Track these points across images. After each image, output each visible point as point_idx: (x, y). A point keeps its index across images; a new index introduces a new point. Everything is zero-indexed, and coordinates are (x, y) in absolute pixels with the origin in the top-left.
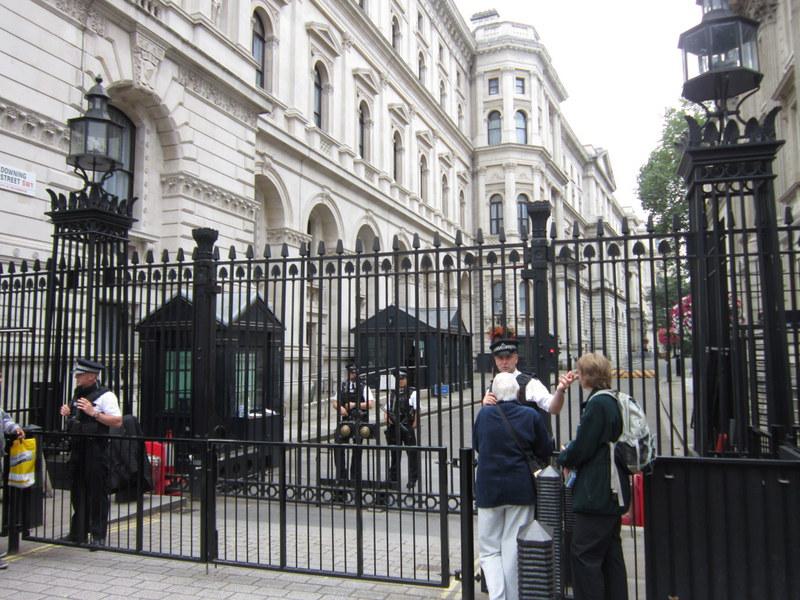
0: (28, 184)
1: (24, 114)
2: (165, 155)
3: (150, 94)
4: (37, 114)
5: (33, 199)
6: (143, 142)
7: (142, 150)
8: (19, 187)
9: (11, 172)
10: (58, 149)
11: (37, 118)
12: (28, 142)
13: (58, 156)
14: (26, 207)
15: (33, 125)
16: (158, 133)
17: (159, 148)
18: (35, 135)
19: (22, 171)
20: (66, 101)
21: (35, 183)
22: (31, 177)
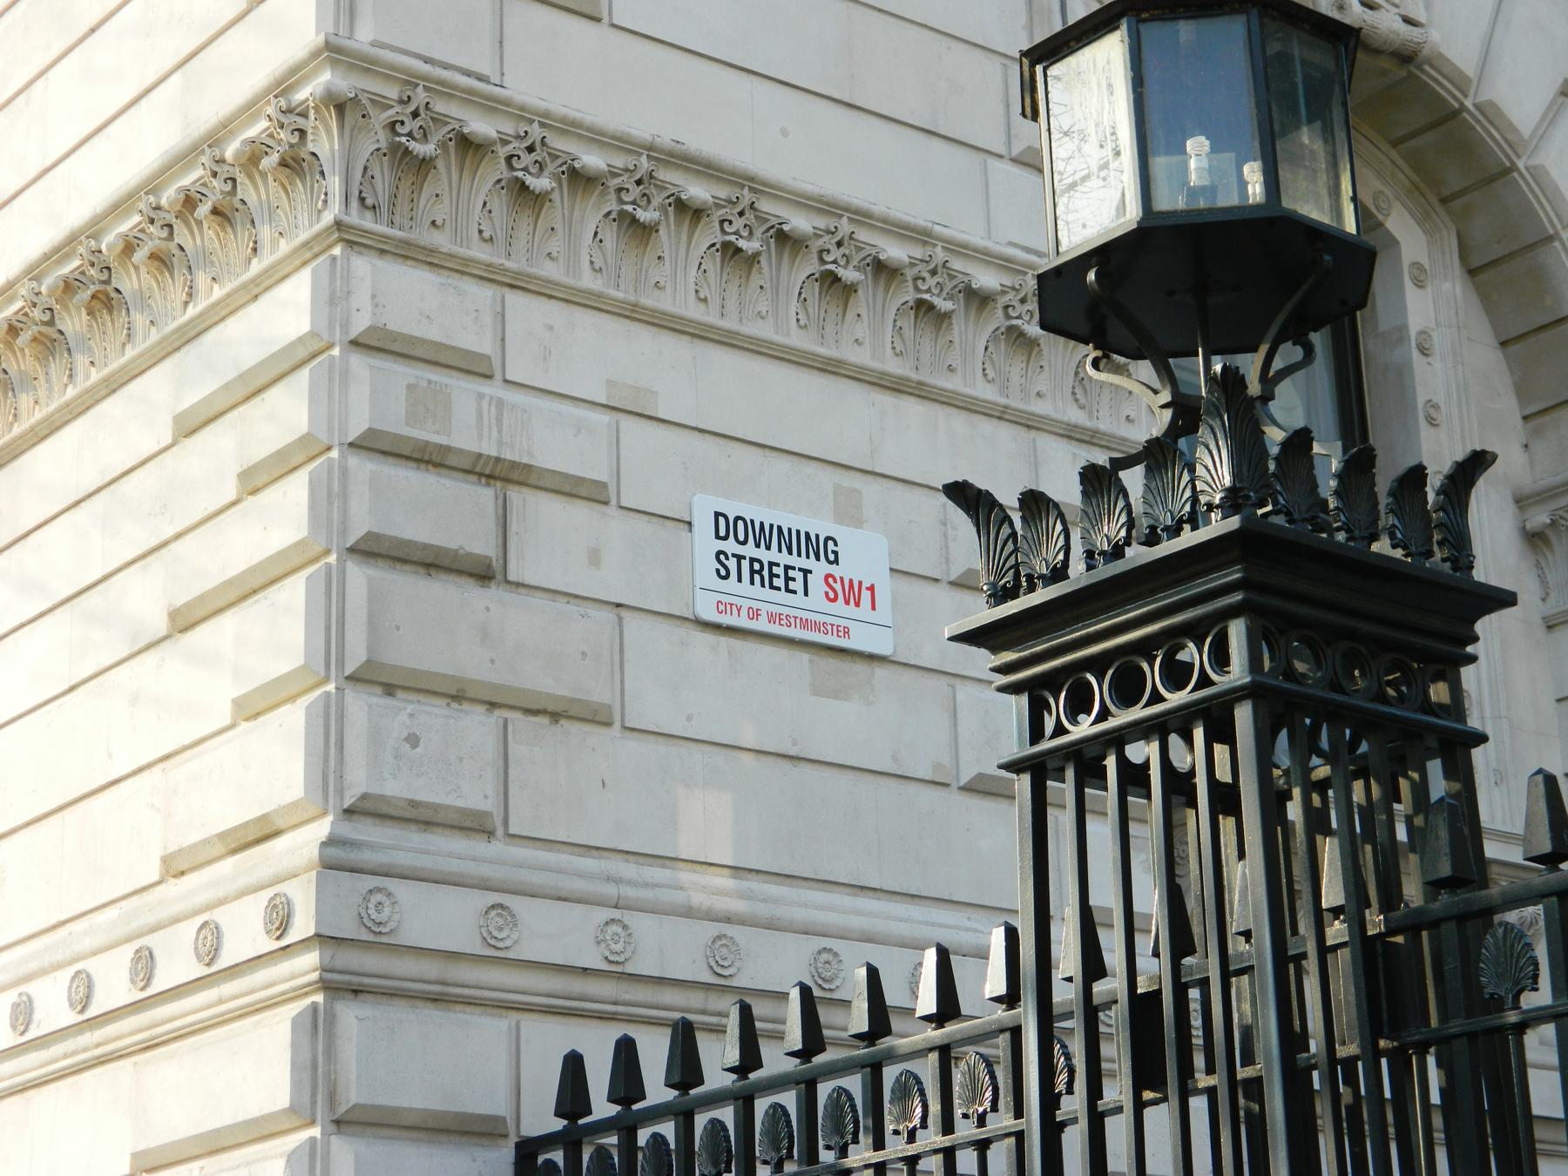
0: (852, 593)
1: (800, 222)
2: (1522, 392)
3: (1406, 57)
4: (862, 216)
5: (881, 672)
6: (1401, 331)
7: (1402, 376)
8: (813, 605)
9: (762, 534)
10: (985, 392)
11: (863, 235)
12: (831, 368)
13: (986, 426)
14: (850, 723)
15: (849, 275)
16: (1472, 272)
17: (1486, 356)
18: (862, 330)
19: (820, 527)
20: (1002, 150)
21: (885, 587)
22: (863, 555)
